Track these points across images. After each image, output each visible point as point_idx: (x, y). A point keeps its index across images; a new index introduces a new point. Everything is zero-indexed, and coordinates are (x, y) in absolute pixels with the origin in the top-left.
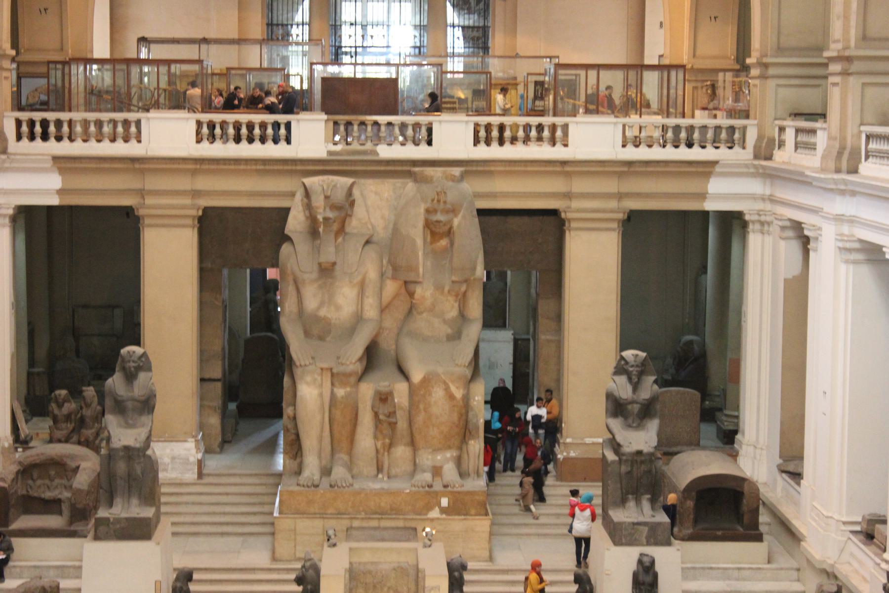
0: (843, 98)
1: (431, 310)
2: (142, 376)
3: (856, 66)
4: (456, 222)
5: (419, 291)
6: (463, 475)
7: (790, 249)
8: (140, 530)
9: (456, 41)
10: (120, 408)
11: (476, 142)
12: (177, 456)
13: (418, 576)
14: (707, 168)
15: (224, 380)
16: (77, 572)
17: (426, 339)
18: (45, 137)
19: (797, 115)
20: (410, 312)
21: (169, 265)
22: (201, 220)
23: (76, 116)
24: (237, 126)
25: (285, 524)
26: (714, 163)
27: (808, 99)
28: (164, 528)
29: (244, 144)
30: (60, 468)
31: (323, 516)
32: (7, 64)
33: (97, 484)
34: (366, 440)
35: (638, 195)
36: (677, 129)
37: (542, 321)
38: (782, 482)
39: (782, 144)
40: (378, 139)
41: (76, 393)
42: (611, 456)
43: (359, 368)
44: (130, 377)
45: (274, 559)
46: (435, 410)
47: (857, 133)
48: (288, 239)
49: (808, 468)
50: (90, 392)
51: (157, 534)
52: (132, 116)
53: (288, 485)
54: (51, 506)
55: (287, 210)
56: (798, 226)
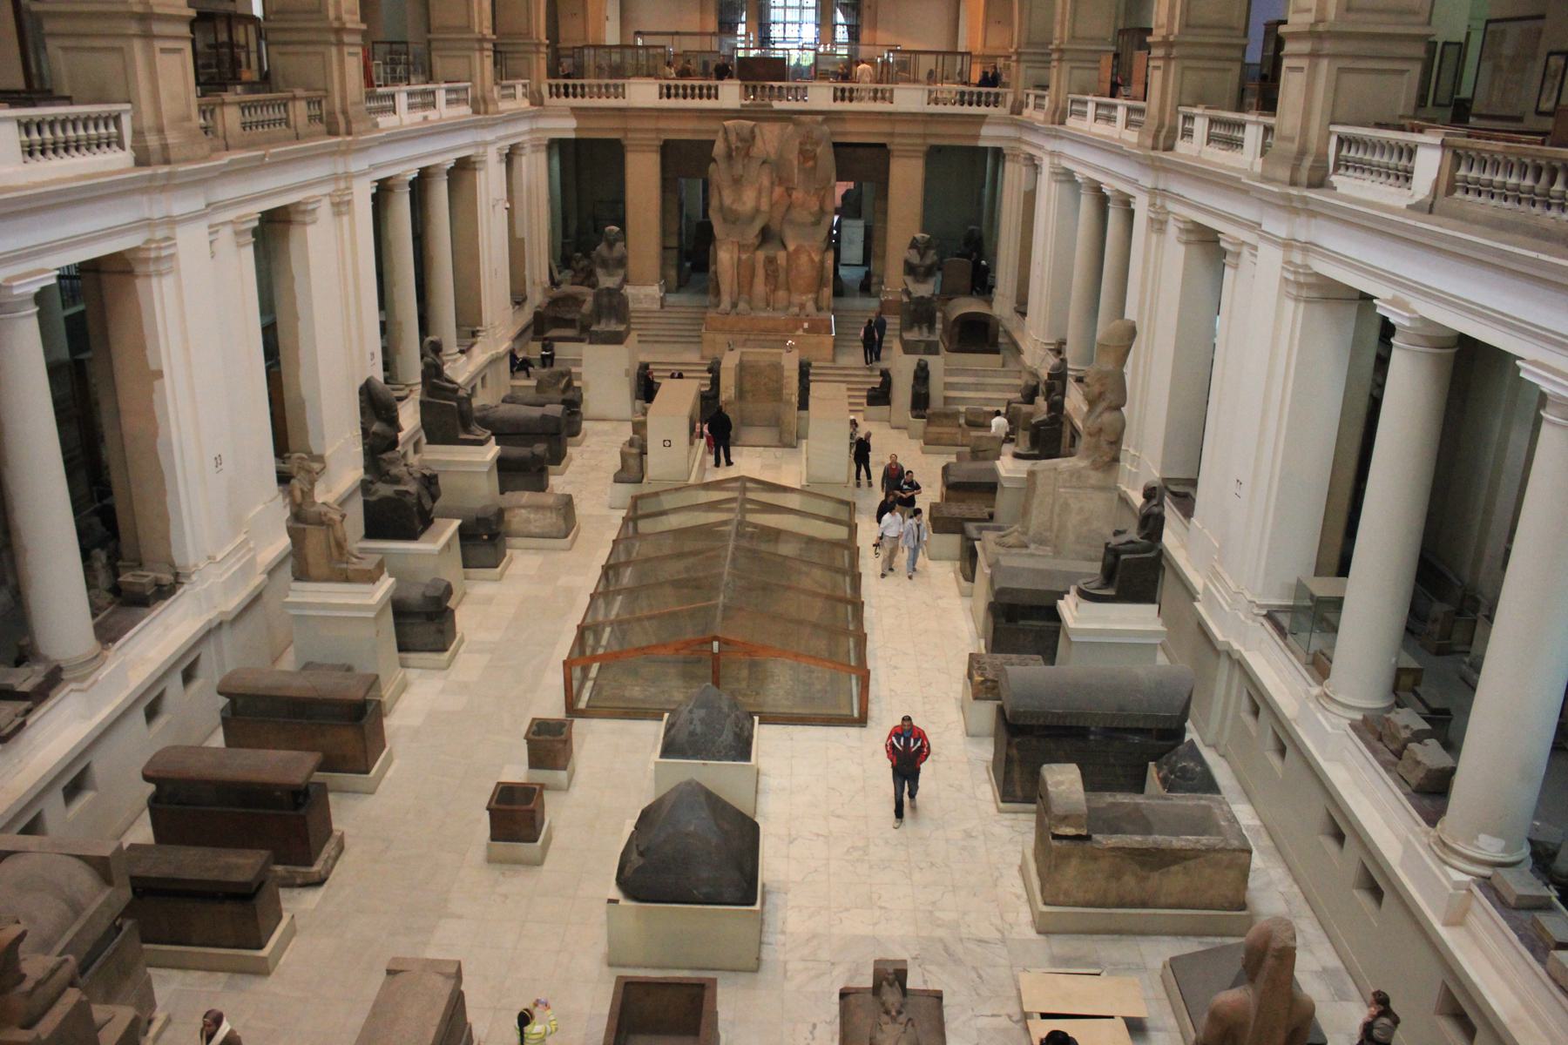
0: (1058, 75)
2: (619, 246)
3: (1066, 56)
4: (819, 150)
5: (795, 194)
6: (819, 309)
8: (616, 339)
9: (842, 34)
10: (605, 264)
11: (835, 100)
12: (645, 294)
13: (777, 368)
18: (567, 95)
20: (789, 208)
21: (642, 176)
23: (585, 82)
24: (685, 88)
25: (708, 336)
26: (984, 116)
28: (633, 336)
29: (689, 100)
30: (576, 301)
31: (731, 332)
32: (543, 49)
34: (760, 287)
35: (936, 136)
38: (1017, 317)
40: (771, 98)
41: (587, 255)
42: (905, 299)
43: (757, 242)
44: (611, 245)
45: (703, 358)
48: (714, 160)
49: (1032, 308)
51: (627, 341)
52: (619, 82)
54: (570, 323)
56: (1031, 158)
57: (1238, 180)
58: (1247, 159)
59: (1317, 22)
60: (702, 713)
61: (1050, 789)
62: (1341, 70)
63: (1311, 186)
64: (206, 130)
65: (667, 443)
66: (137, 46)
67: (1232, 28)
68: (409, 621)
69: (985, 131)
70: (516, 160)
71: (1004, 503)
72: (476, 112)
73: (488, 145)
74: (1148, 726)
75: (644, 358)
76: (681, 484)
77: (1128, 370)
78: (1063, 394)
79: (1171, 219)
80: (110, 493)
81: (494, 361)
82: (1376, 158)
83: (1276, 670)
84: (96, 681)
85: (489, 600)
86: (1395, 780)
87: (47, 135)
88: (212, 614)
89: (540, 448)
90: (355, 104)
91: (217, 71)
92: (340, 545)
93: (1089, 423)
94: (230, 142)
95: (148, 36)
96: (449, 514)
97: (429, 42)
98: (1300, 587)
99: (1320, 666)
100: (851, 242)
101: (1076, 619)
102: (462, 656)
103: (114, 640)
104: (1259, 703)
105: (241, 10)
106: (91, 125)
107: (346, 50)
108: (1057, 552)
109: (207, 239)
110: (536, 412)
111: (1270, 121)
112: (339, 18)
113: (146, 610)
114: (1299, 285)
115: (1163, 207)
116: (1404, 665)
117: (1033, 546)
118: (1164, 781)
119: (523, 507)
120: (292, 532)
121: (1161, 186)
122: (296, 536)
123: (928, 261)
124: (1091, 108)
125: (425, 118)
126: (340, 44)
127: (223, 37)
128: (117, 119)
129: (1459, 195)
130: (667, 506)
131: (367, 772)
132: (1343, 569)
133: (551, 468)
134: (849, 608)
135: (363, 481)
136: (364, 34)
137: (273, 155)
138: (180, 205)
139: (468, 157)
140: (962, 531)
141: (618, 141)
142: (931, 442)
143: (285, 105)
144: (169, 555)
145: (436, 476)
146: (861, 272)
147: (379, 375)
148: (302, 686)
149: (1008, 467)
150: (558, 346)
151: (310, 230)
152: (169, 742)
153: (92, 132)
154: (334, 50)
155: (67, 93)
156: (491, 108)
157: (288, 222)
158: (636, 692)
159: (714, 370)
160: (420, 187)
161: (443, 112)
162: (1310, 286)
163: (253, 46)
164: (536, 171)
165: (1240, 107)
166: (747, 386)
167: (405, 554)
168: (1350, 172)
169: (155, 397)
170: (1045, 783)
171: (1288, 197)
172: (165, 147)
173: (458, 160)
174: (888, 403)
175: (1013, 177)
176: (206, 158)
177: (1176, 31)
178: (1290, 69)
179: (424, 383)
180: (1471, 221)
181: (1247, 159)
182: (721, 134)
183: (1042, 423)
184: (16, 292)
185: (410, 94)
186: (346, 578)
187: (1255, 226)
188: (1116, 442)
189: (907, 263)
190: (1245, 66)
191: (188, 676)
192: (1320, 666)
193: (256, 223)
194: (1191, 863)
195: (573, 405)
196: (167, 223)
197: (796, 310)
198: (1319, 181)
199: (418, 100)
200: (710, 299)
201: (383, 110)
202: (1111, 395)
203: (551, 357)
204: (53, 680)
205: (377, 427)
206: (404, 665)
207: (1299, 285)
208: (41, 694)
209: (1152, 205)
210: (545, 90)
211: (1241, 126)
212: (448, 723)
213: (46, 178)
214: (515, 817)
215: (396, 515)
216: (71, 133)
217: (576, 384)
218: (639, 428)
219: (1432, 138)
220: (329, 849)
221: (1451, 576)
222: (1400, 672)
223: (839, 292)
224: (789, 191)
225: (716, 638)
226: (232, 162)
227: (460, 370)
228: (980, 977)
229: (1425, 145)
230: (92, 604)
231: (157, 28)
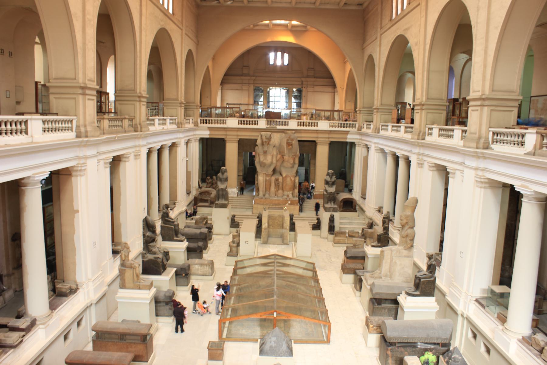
0: (377, 117)
1: (288, 161)
2: (225, 173)
3: (379, 110)
4: (293, 142)
5: (285, 157)
6: (293, 197)
7: (364, 150)
8: (224, 206)
9: (294, 106)
10: (221, 180)
12: (233, 191)
13: (283, 217)
14: (347, 132)
16: (211, 215)
17: (286, 168)
18: (206, 123)
19: (367, 121)
21: (232, 152)
22: (239, 141)
23: (213, 119)
24: (247, 121)
25: (255, 206)
27: (369, 118)
28: (230, 206)
30: (208, 193)
31: (263, 204)
32: (199, 107)
33: (216, 196)
34: (273, 189)
37: (311, 165)
38: (361, 200)
39: (363, 128)
40: (277, 124)
41: (212, 178)
42: (325, 193)
43: (272, 173)
44: (223, 174)
45: (253, 213)
46: (288, 183)
47: (380, 125)
48: (257, 145)
49: (367, 197)
50: (214, 177)
52: (225, 119)
53: (256, 198)
54: (206, 201)
55: (256, 140)
56: (366, 145)
57: (456, 148)
59: (482, 95)
63: (484, 148)
65: (247, 242)
66: (81, 97)
68: (159, 305)
69: (349, 136)
70: (189, 144)
71: (369, 264)
72: (178, 127)
73: (180, 138)
74: (438, 342)
75: (233, 213)
78: (389, 224)
79: (426, 163)
82: (509, 138)
89: (201, 244)
92: (138, 276)
93: (403, 233)
94: (105, 132)
95: (84, 94)
96: (172, 266)
105: (103, 90)
107: (142, 103)
110: (198, 231)
111: (464, 128)
112: (140, 93)
114: (482, 182)
117: (383, 278)
119: (196, 265)
122: (122, 273)
124: (390, 128)
126: (140, 101)
128: (71, 121)
130: (246, 265)
131: (147, 361)
133: (204, 251)
134: (316, 300)
137: (118, 137)
140: (355, 273)
145: (168, 252)
148: (123, 328)
151: (127, 164)
155: (55, 112)
156: (183, 126)
157: (120, 161)
162: (485, 183)
163: (107, 103)
164: (195, 148)
166: (271, 223)
169: (75, 219)
171: (476, 153)
172: (86, 132)
174: (319, 229)
175: (359, 153)
176: (98, 136)
177: (424, 100)
178: (473, 110)
182: (260, 136)
183: (381, 234)
184: (36, 179)
185: (159, 120)
187: (462, 164)
188: (413, 240)
193: (111, 160)
195: (210, 228)
196: (84, 158)
197: (286, 197)
199: (161, 122)
201: (150, 125)
202: (409, 224)
205: (148, 234)
206: (157, 322)
207: (482, 182)
208: (28, 330)
210: (199, 121)
211: (452, 130)
213: (48, 140)
215: (152, 267)
218: (237, 236)
224: (283, 156)
225: (276, 311)
226: (107, 138)
227: (173, 214)
231: (88, 92)
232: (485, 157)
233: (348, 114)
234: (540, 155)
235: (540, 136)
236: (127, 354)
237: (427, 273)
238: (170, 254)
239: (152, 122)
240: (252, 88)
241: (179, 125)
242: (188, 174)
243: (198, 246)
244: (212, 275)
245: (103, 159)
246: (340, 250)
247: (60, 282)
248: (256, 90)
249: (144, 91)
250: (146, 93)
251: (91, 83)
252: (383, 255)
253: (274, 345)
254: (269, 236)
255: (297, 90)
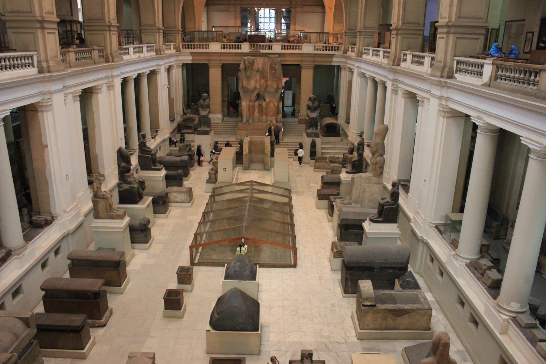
0: (359, 40)
2: (207, 100)
3: (362, 34)
4: (277, 67)
5: (268, 82)
6: (277, 122)
8: (206, 133)
9: (284, 27)
10: (202, 107)
12: (216, 117)
13: (263, 143)
15: (228, 101)
18: (188, 48)
19: (352, 44)
20: (266, 87)
21: (215, 76)
23: (195, 43)
24: (230, 45)
25: (239, 132)
26: (334, 55)
30: (192, 120)
31: (246, 130)
32: (180, 32)
34: (256, 114)
35: (317, 61)
36: (326, 47)
38: (346, 124)
41: (196, 104)
42: (307, 118)
44: (204, 100)
48: (240, 70)
54: (190, 128)
55: (240, 64)
56: (350, 69)
57: (423, 76)
58: (425, 69)
59: (449, 22)
60: (238, 264)
61: (361, 289)
62: (457, 38)
64: (63, 61)
65: (225, 169)
66: (39, 31)
67: (419, 24)
69: (335, 60)
72: (157, 54)
73: (161, 66)
74: (395, 266)
75: (216, 140)
76: (230, 184)
77: (385, 142)
78: (363, 151)
79: (399, 90)
80: (29, 188)
81: (164, 141)
83: (439, 246)
84: (24, 255)
85: (163, 225)
86: (482, 284)
87: (7, 63)
88: (65, 231)
89: (180, 171)
90: (115, 51)
91: (66, 41)
92: (110, 206)
93: (372, 160)
95: (43, 28)
96: (149, 195)
97: (140, 30)
98: (447, 217)
99: (454, 244)
100: (288, 99)
101: (369, 229)
102: (154, 245)
103: (30, 240)
104: (433, 257)
105: (75, 19)
106: (23, 59)
107: (112, 33)
108: (362, 206)
109: (64, 99)
110: (179, 159)
111: (433, 55)
112: (109, 22)
113: (42, 230)
114: (444, 112)
115: (397, 85)
116: (483, 243)
117: (353, 204)
118: (401, 285)
120: (94, 202)
121: (396, 78)
123: (315, 105)
124: (371, 52)
125: (139, 56)
126: (110, 31)
127: (69, 28)
128: (32, 57)
129: (499, 80)
130: (225, 191)
131: (121, 286)
132: (462, 210)
135: (118, 183)
136: (118, 27)
137: (86, 69)
138: (54, 87)
139: (154, 70)
141: (207, 64)
142: (317, 168)
143: (91, 52)
144: (50, 209)
145: (144, 182)
146: (292, 109)
147: (124, 146)
148: (96, 256)
149: (344, 176)
150: (186, 135)
151: (99, 95)
152: (49, 276)
153: (23, 61)
154: (108, 33)
155: (14, 48)
156: (162, 53)
157: (92, 93)
158: (215, 257)
159: (241, 144)
160: (138, 80)
161: (146, 54)
162: (448, 112)
164: (178, 74)
165: (423, 51)
166: (253, 149)
167: (133, 209)
168: (461, 73)
169: (45, 154)
170: (359, 286)
171: (440, 82)
172: (49, 67)
173: (151, 71)
175: (344, 76)
176: (63, 71)
177: (400, 25)
179: (139, 148)
180: (504, 90)
181: (425, 69)
182: (242, 61)
183: (356, 161)
185: (134, 48)
186: (113, 218)
187: (429, 92)
188: (382, 167)
189: (308, 105)
190: (424, 37)
191: (57, 253)
192: (454, 244)
193: (81, 93)
194: (411, 314)
196: (50, 93)
198: (451, 76)
199: (137, 50)
200: (239, 119)
201: (124, 54)
202: (380, 150)
203: (184, 139)
204: (9, 254)
205: (123, 164)
207: (444, 112)
209: (393, 85)
210: (181, 46)
211: (423, 57)
212: (149, 268)
214: (173, 301)
215: (129, 196)
216: (16, 62)
217: (193, 149)
218: (215, 164)
219: (489, 61)
220: (107, 314)
221: (499, 212)
222: (482, 246)
223: (284, 116)
224: (266, 81)
225: (243, 237)
226: (72, 72)
227: (152, 144)
228: (338, 355)
229: (487, 63)
230: (22, 227)
231: (46, 25)
232: (448, 87)
233: (335, 35)
234: (494, 87)
235: (495, 67)
236: (97, 280)
237: (390, 201)
238: (146, 183)
239: (127, 51)
240: (238, 9)
241: (158, 52)
242: (171, 101)
243: (178, 174)
244: (190, 202)
245: (72, 93)
246: (319, 175)
247: (36, 215)
248: (243, 10)
249: (113, 20)
250: (116, 21)
251: (50, 16)
252: (354, 182)
253: (238, 269)
254: (251, 162)
255: (286, 11)
